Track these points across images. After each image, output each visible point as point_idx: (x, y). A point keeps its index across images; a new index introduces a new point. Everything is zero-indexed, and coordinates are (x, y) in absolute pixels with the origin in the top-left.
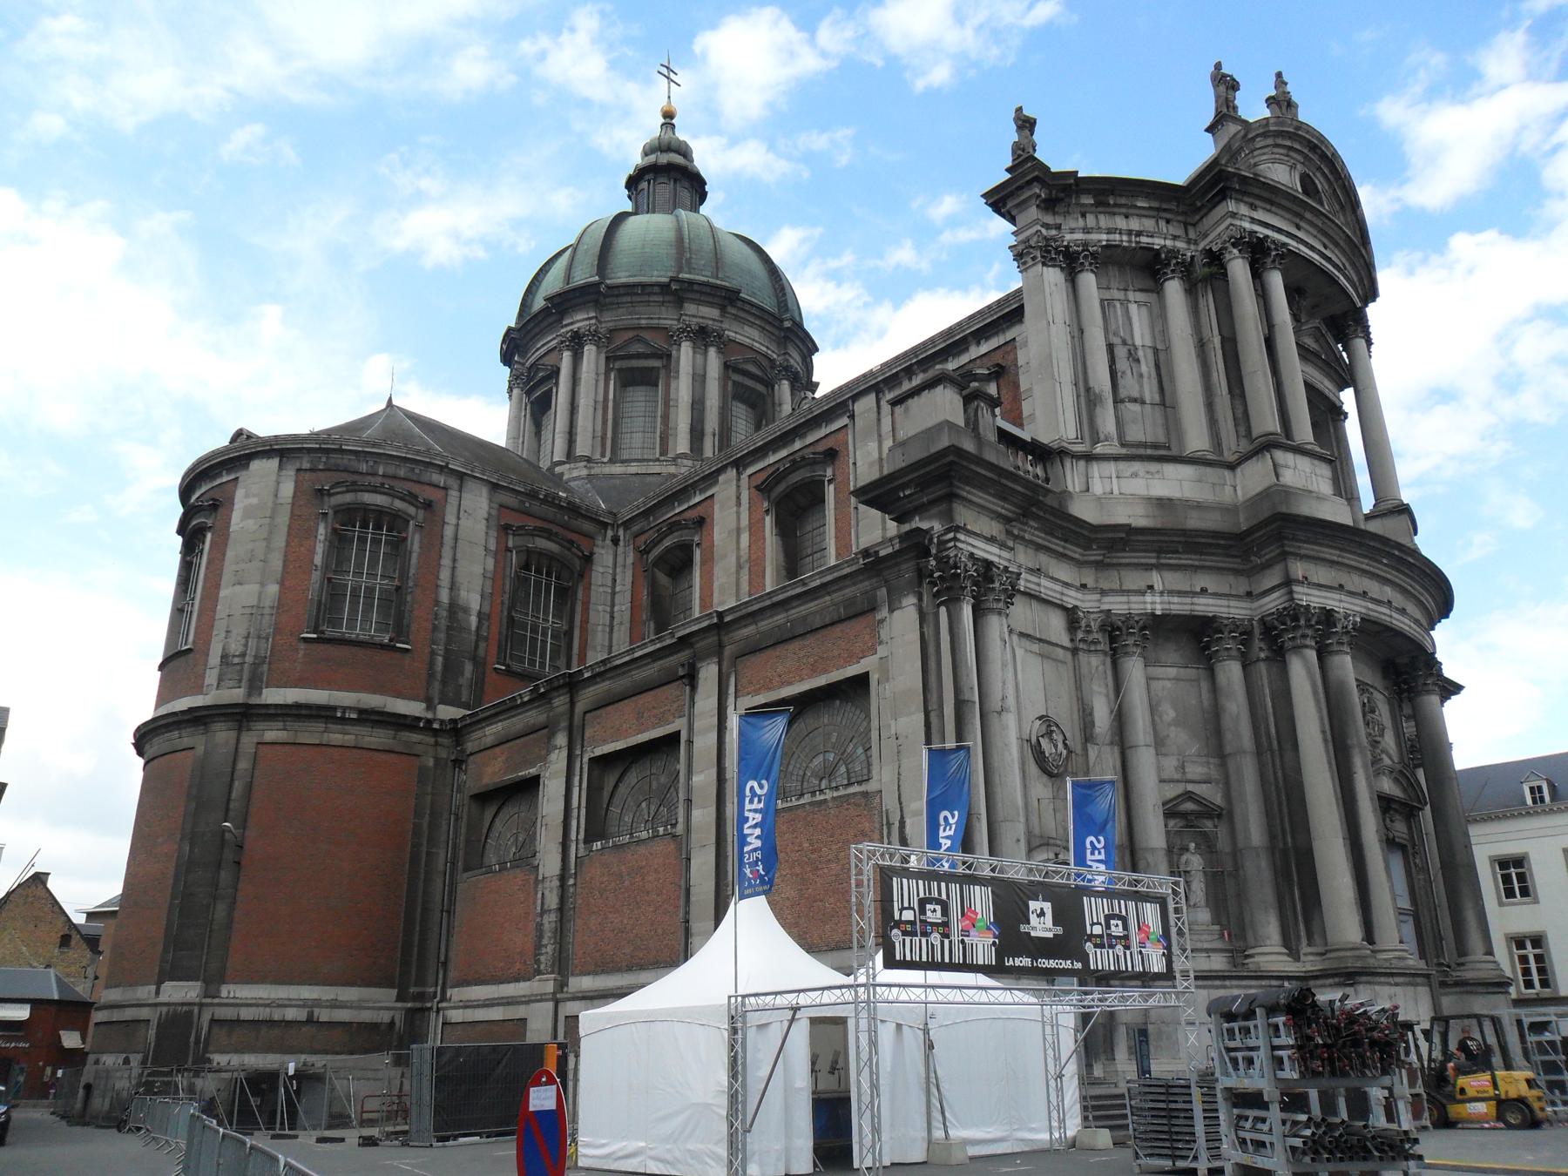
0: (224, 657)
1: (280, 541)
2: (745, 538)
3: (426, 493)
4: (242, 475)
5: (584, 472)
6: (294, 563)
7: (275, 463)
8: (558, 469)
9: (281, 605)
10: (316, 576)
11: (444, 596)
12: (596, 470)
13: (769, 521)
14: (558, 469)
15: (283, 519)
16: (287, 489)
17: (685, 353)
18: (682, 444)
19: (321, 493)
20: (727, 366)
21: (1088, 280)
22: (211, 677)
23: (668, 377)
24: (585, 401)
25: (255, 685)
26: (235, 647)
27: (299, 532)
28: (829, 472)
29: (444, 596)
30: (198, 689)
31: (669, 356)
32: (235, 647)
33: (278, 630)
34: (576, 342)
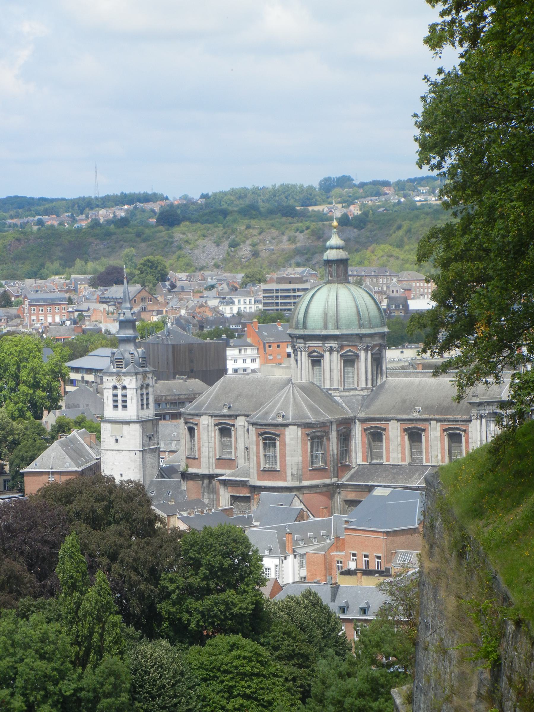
0: (292, 474)
1: (300, 446)
2: (399, 439)
3: (326, 429)
4: (287, 429)
5: (338, 394)
6: (304, 451)
7: (296, 427)
8: (330, 392)
9: (303, 462)
10: (309, 455)
11: (331, 453)
12: (342, 394)
13: (406, 437)
14: (330, 392)
15: (300, 441)
16: (300, 433)
17: (362, 354)
18: (364, 386)
19: (308, 435)
20: (372, 354)
21: (484, 421)
22: (289, 478)
23: (358, 362)
24: (335, 371)
25: (300, 481)
26: (295, 472)
27: (304, 444)
28: (423, 433)
29: (331, 453)
30: (285, 480)
31: (357, 356)
32: (295, 472)
33: (303, 467)
34: (331, 350)
